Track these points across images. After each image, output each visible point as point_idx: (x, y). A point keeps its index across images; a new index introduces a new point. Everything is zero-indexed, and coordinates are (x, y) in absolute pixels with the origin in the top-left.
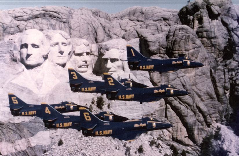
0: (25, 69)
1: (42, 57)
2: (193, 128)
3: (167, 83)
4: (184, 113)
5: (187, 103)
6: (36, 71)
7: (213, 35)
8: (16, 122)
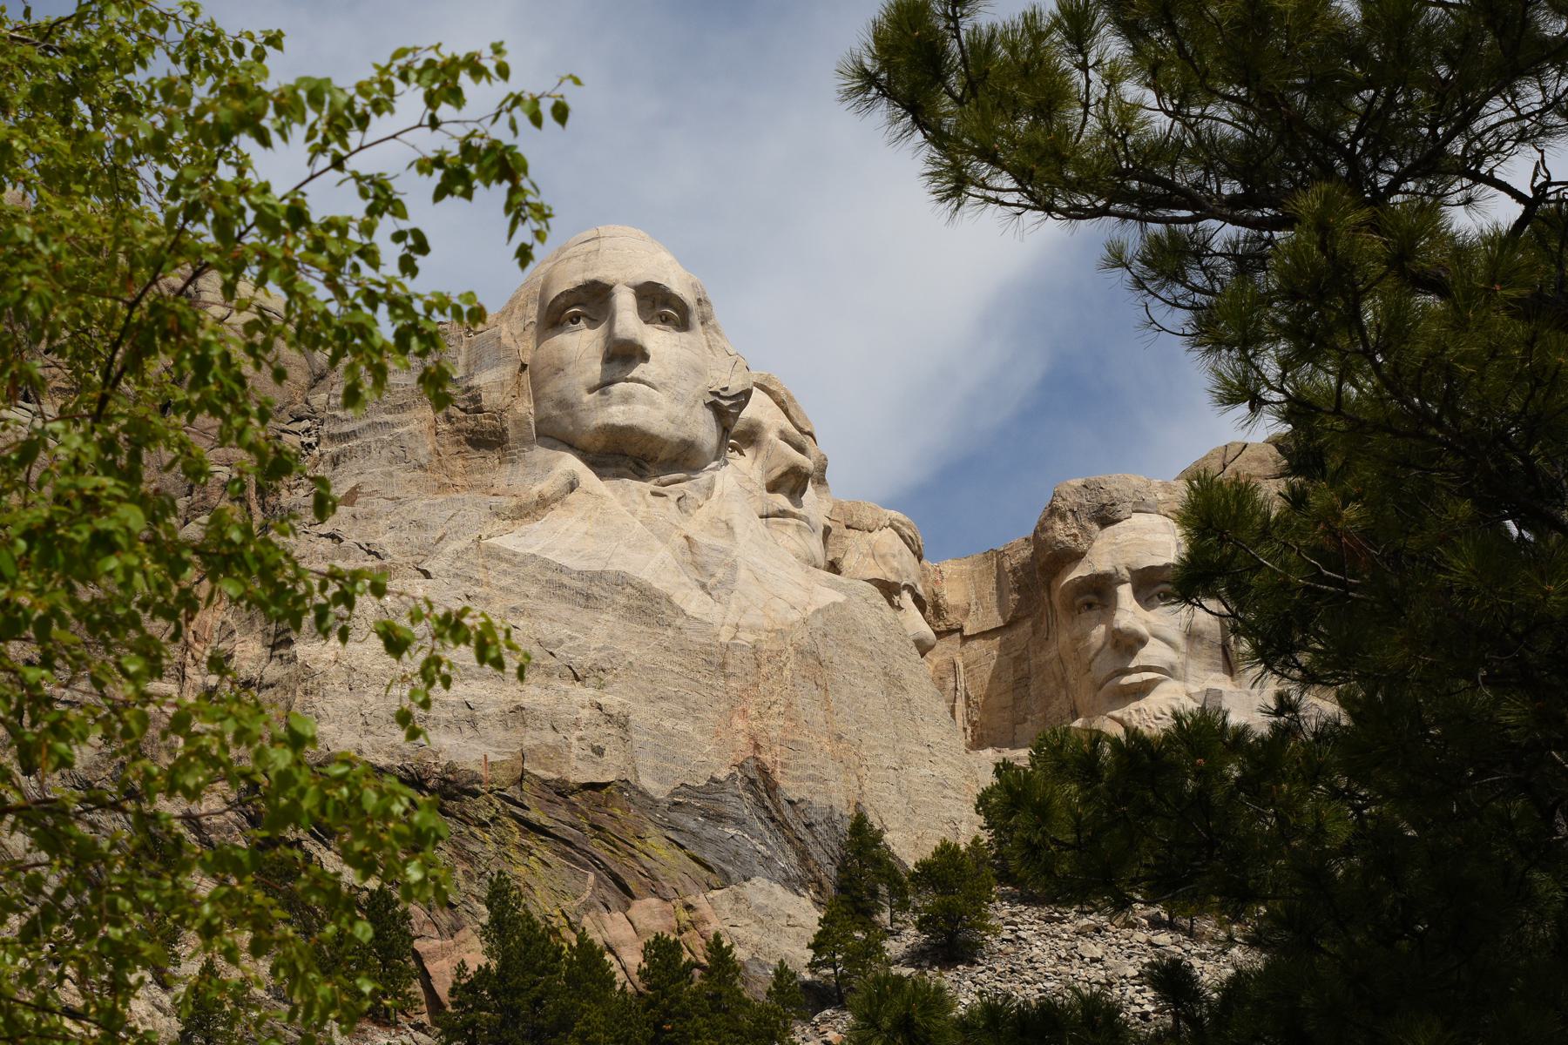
6: (673, 497)
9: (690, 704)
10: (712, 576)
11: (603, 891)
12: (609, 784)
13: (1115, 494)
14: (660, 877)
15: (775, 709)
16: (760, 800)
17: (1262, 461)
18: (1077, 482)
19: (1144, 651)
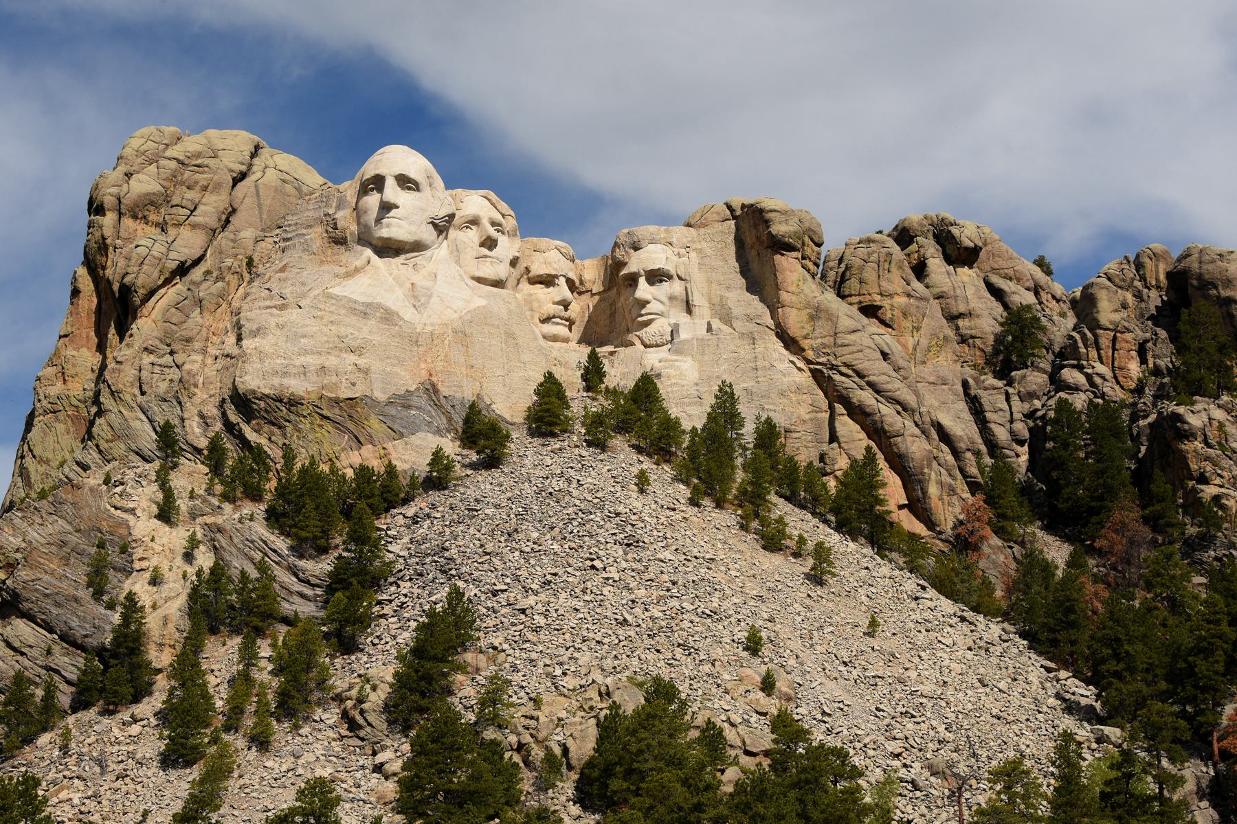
0: (374, 258)
2: (923, 474)
3: (832, 339)
4: (891, 425)
5: (898, 403)
7: (962, 308)
8: (343, 396)
16: (430, 397)
17: (718, 213)
18: (626, 231)
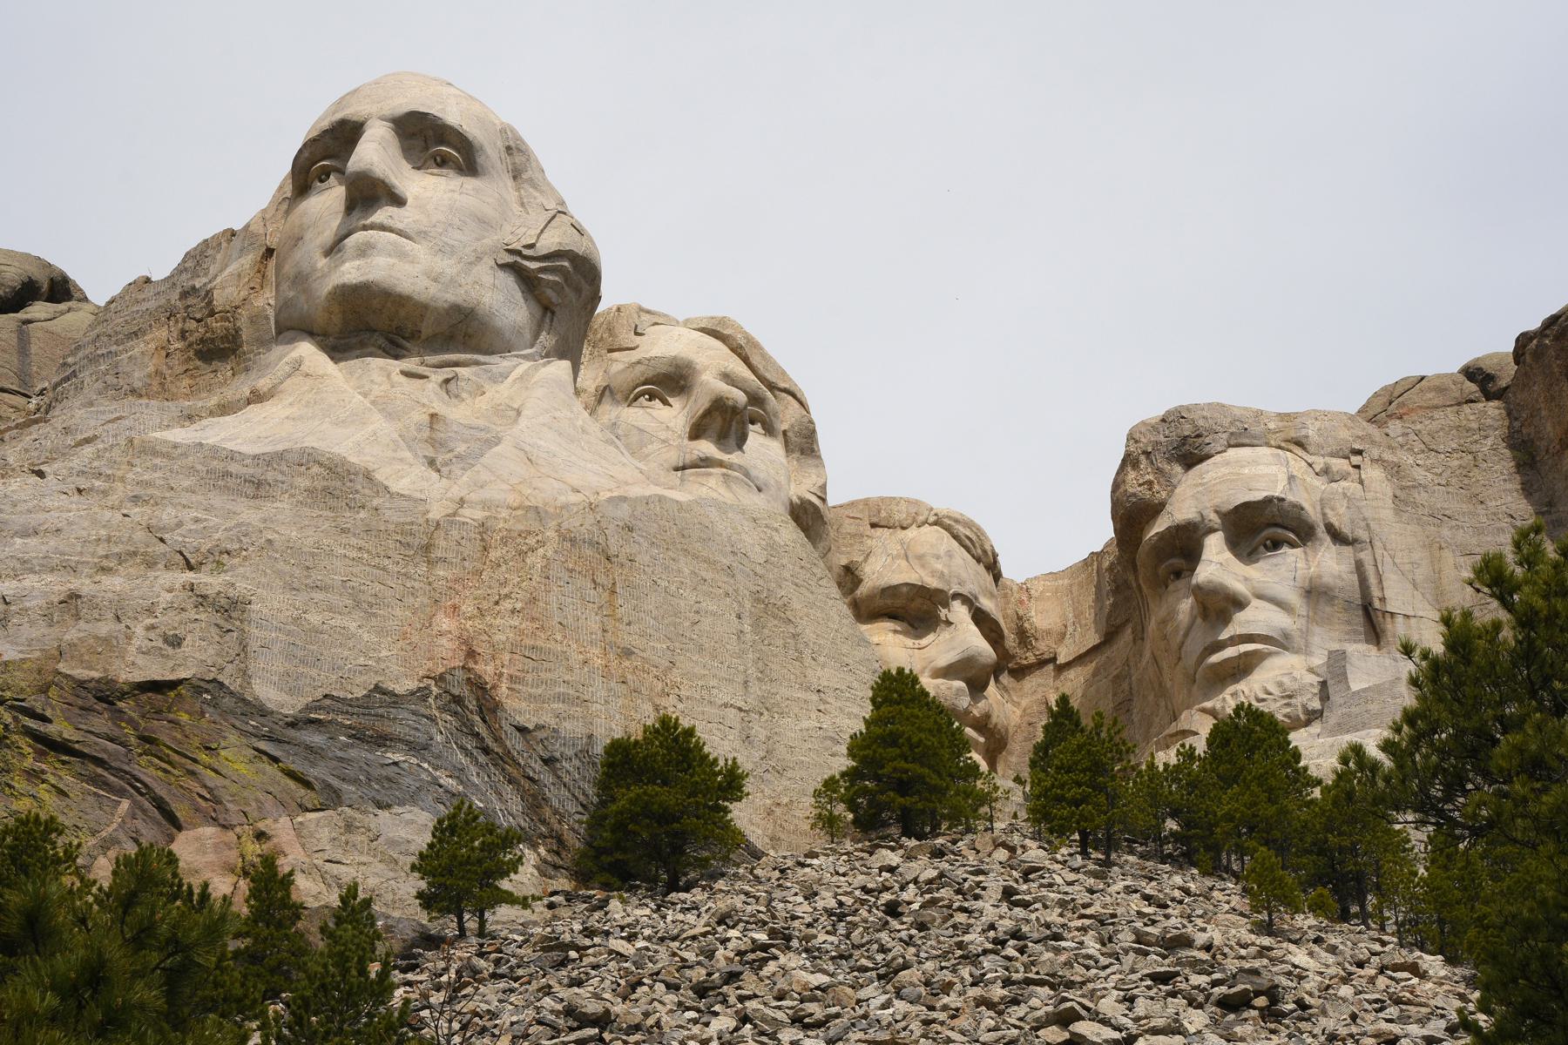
1: (504, 267)
9: (362, 597)
10: (451, 451)
11: (139, 824)
12: (180, 682)
13: (1201, 423)
14: (226, 798)
15: (507, 605)
19: (1240, 617)
